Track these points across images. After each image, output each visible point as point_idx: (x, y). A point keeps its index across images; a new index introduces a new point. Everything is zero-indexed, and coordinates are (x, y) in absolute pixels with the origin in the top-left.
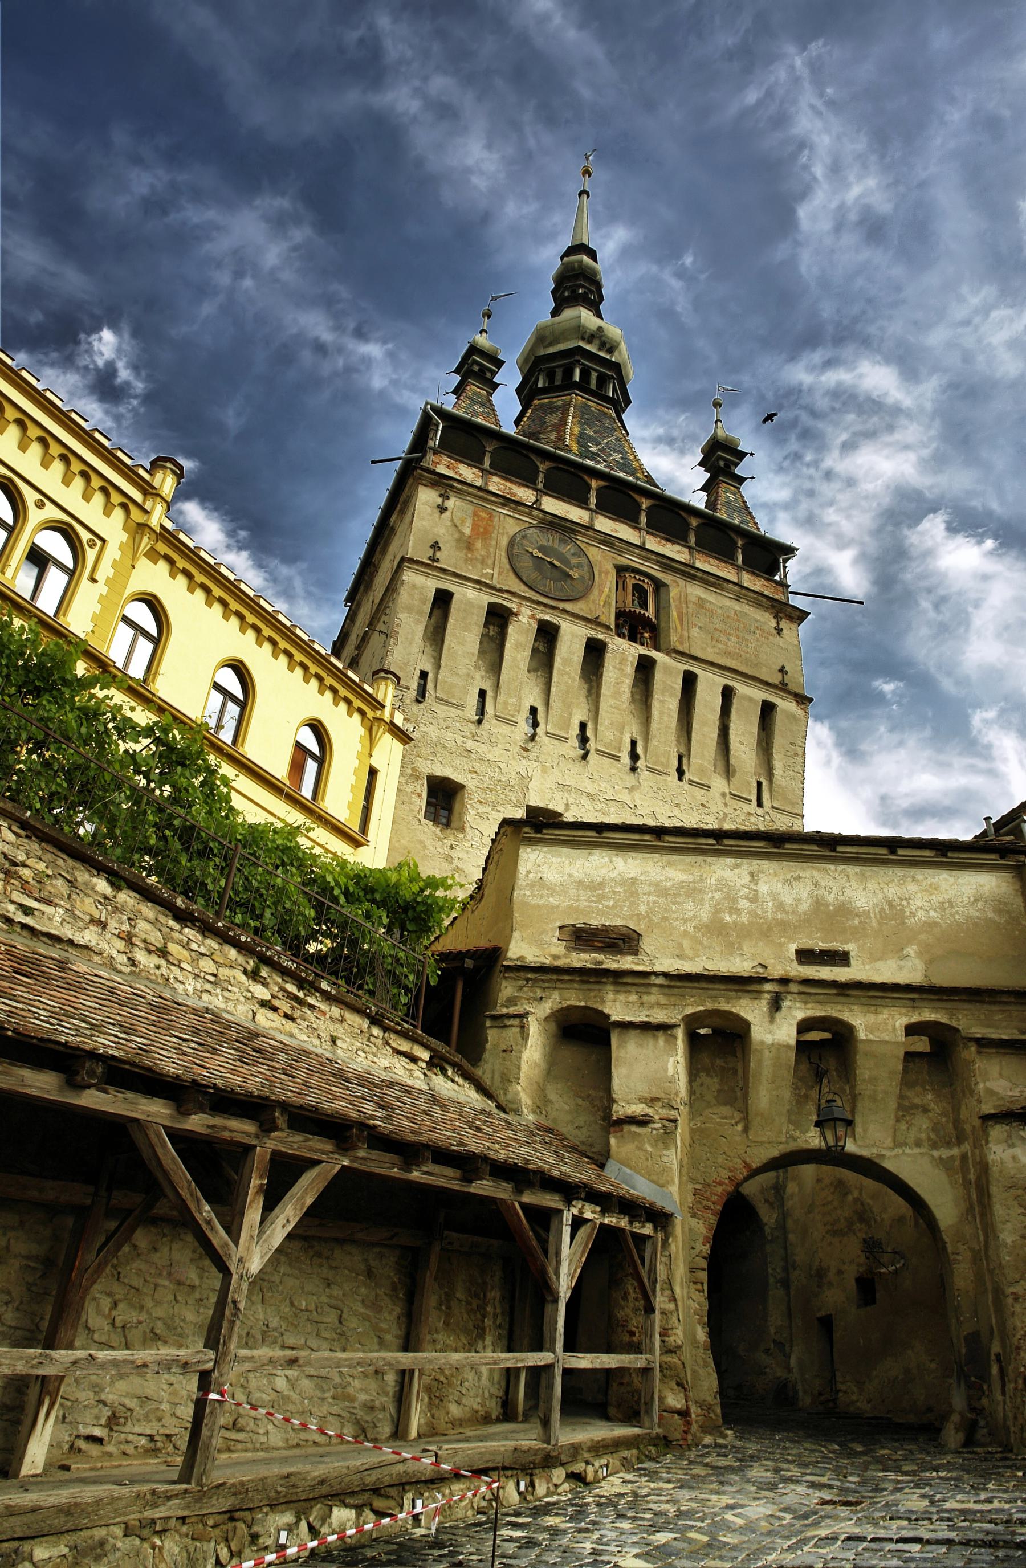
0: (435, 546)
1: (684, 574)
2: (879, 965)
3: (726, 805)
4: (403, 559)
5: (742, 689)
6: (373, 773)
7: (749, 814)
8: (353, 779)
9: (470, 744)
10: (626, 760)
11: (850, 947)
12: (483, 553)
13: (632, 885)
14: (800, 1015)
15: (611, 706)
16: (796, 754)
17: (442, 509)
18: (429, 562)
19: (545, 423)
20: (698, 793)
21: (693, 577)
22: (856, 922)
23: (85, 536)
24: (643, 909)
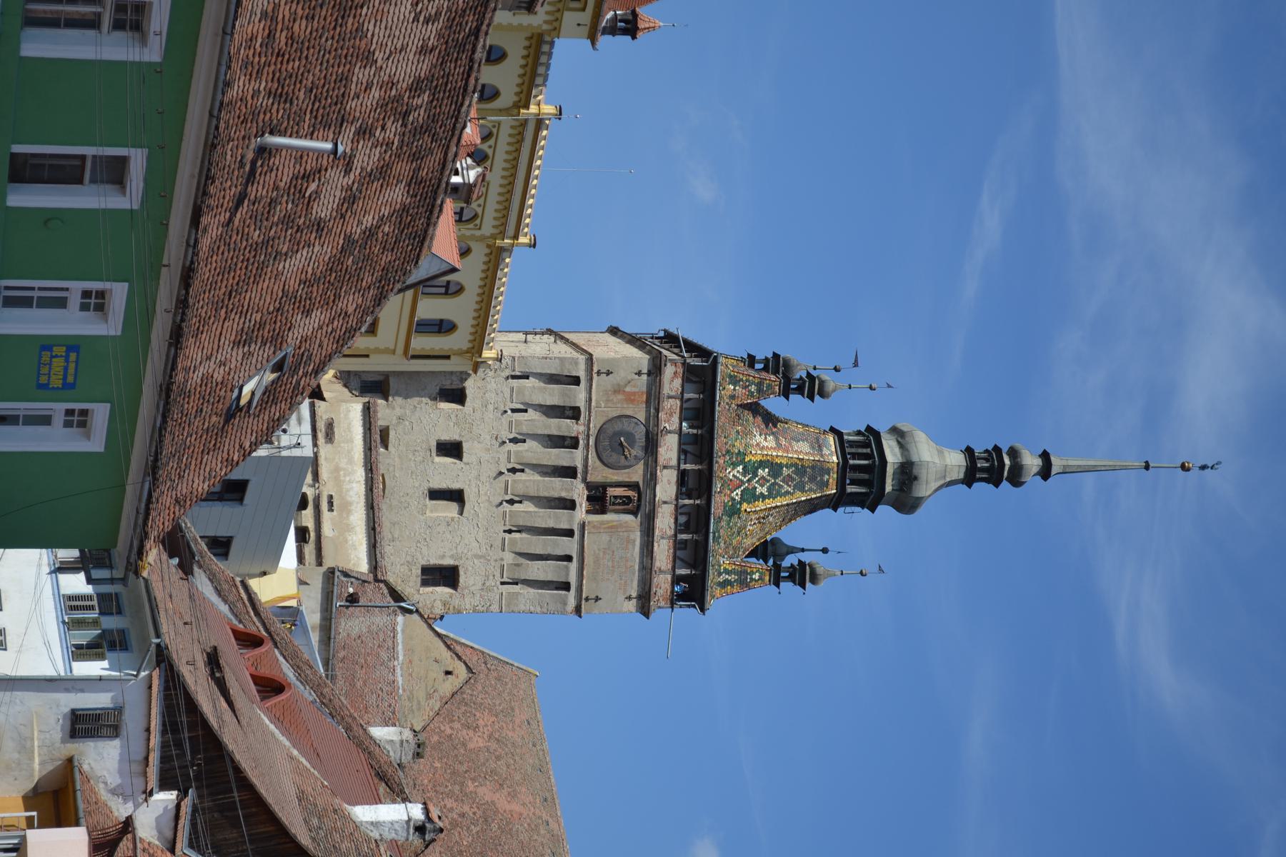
0: (608, 373)
1: (649, 528)
2: (329, 522)
3: (496, 561)
4: (591, 355)
5: (574, 566)
6: (448, 357)
7: (494, 576)
8: (437, 348)
9: (491, 407)
10: (508, 498)
11: (335, 513)
12: (615, 400)
13: (351, 441)
14: (308, 493)
15: (538, 486)
16: (541, 608)
17: (639, 373)
18: (595, 369)
19: (798, 441)
20: (499, 543)
21: (648, 536)
22: (345, 516)
23: (478, 222)
24: (342, 445)
